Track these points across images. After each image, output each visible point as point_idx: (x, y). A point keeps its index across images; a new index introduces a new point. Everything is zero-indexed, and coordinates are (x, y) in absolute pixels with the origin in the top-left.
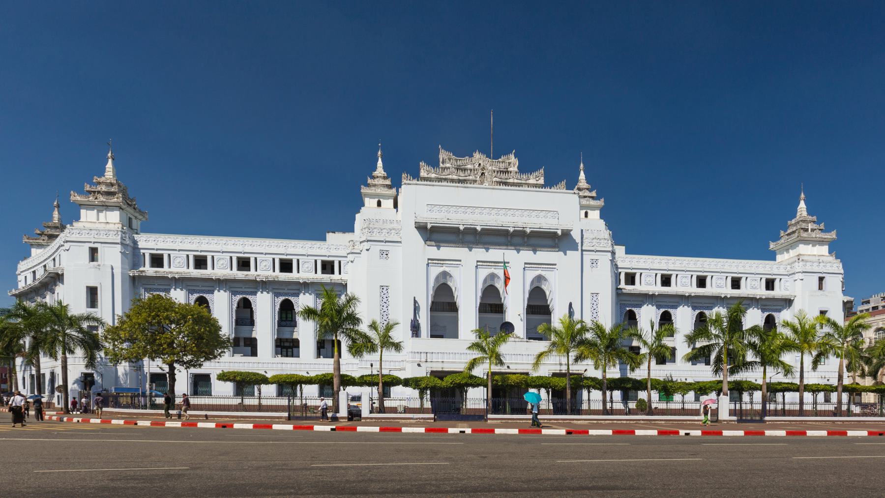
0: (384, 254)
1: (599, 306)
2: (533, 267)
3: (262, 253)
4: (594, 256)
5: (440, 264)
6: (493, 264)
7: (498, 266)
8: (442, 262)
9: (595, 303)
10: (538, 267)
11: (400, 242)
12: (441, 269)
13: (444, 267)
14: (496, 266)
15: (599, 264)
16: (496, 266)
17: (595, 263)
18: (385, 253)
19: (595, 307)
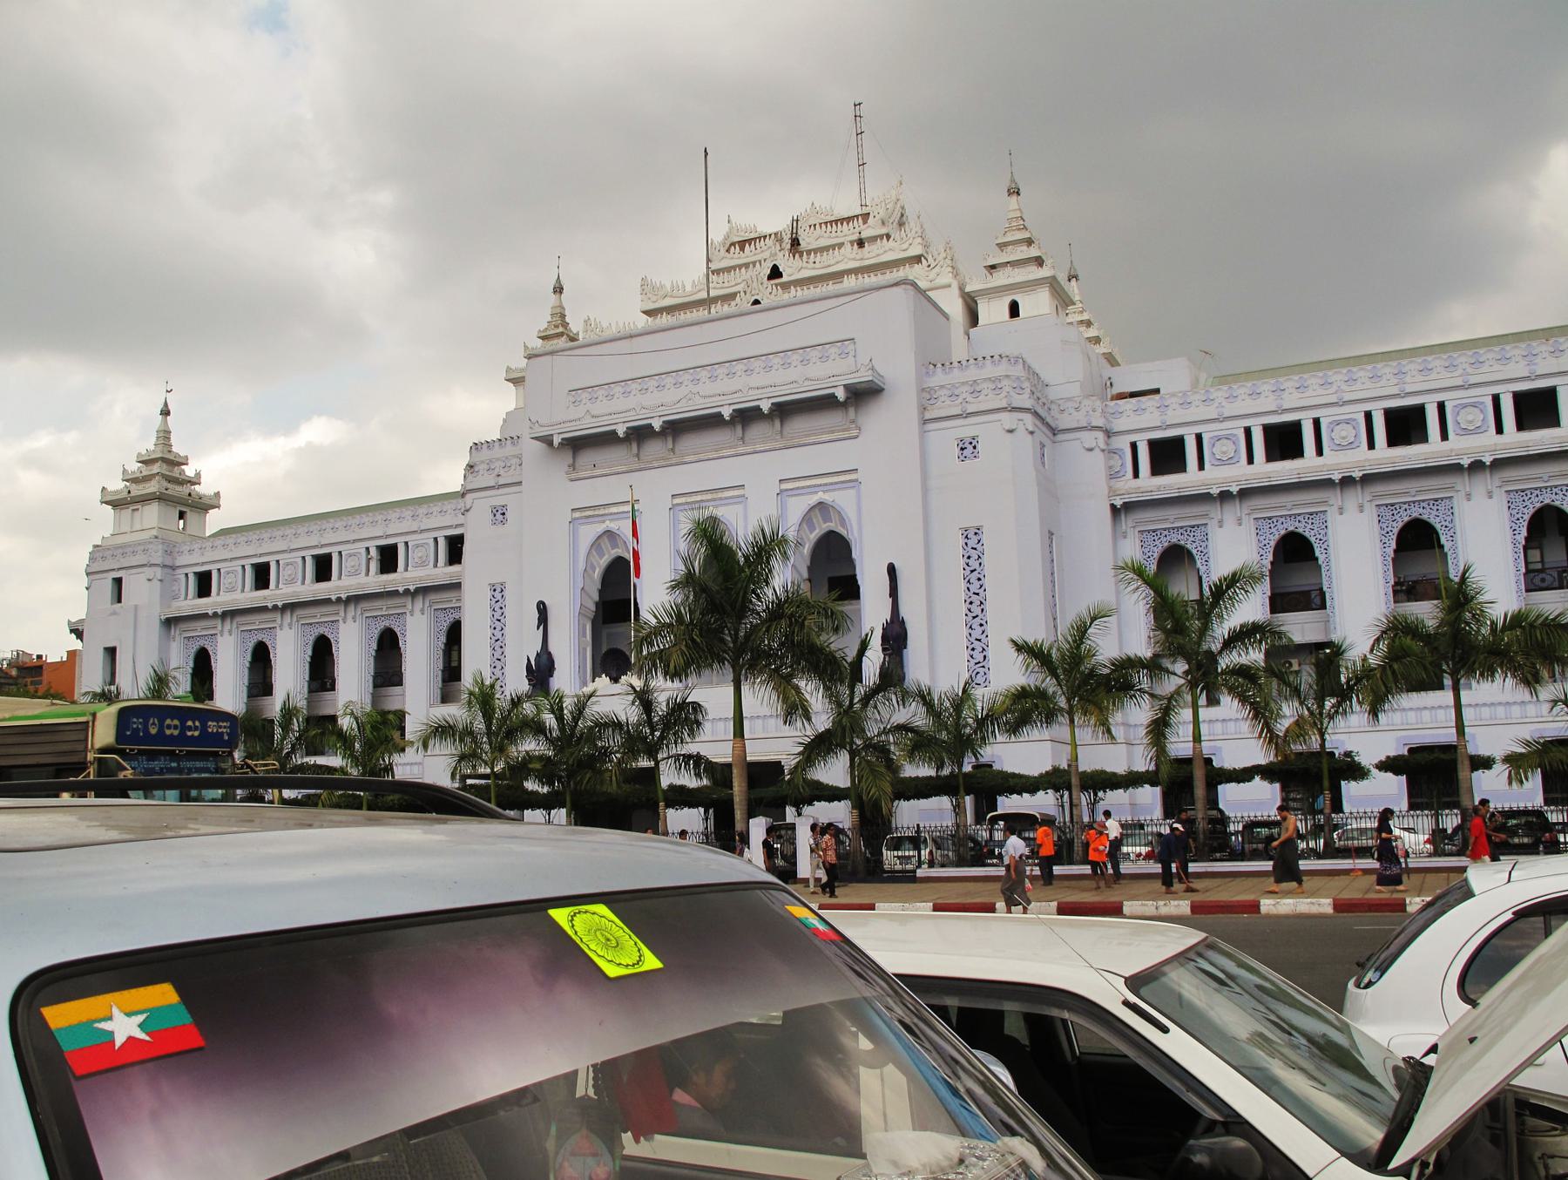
0: (498, 515)
1: (985, 559)
2: (803, 488)
3: (348, 542)
4: (966, 429)
5: (598, 516)
6: (709, 496)
7: (721, 499)
8: (602, 512)
9: (974, 554)
10: (815, 486)
11: (520, 483)
12: (601, 528)
13: (608, 522)
14: (714, 500)
15: (979, 447)
16: (714, 500)
17: (971, 447)
18: (500, 511)
19: (974, 564)
